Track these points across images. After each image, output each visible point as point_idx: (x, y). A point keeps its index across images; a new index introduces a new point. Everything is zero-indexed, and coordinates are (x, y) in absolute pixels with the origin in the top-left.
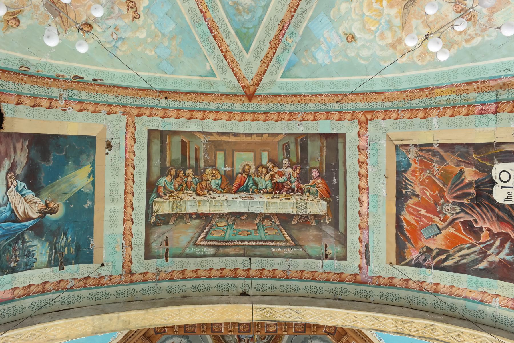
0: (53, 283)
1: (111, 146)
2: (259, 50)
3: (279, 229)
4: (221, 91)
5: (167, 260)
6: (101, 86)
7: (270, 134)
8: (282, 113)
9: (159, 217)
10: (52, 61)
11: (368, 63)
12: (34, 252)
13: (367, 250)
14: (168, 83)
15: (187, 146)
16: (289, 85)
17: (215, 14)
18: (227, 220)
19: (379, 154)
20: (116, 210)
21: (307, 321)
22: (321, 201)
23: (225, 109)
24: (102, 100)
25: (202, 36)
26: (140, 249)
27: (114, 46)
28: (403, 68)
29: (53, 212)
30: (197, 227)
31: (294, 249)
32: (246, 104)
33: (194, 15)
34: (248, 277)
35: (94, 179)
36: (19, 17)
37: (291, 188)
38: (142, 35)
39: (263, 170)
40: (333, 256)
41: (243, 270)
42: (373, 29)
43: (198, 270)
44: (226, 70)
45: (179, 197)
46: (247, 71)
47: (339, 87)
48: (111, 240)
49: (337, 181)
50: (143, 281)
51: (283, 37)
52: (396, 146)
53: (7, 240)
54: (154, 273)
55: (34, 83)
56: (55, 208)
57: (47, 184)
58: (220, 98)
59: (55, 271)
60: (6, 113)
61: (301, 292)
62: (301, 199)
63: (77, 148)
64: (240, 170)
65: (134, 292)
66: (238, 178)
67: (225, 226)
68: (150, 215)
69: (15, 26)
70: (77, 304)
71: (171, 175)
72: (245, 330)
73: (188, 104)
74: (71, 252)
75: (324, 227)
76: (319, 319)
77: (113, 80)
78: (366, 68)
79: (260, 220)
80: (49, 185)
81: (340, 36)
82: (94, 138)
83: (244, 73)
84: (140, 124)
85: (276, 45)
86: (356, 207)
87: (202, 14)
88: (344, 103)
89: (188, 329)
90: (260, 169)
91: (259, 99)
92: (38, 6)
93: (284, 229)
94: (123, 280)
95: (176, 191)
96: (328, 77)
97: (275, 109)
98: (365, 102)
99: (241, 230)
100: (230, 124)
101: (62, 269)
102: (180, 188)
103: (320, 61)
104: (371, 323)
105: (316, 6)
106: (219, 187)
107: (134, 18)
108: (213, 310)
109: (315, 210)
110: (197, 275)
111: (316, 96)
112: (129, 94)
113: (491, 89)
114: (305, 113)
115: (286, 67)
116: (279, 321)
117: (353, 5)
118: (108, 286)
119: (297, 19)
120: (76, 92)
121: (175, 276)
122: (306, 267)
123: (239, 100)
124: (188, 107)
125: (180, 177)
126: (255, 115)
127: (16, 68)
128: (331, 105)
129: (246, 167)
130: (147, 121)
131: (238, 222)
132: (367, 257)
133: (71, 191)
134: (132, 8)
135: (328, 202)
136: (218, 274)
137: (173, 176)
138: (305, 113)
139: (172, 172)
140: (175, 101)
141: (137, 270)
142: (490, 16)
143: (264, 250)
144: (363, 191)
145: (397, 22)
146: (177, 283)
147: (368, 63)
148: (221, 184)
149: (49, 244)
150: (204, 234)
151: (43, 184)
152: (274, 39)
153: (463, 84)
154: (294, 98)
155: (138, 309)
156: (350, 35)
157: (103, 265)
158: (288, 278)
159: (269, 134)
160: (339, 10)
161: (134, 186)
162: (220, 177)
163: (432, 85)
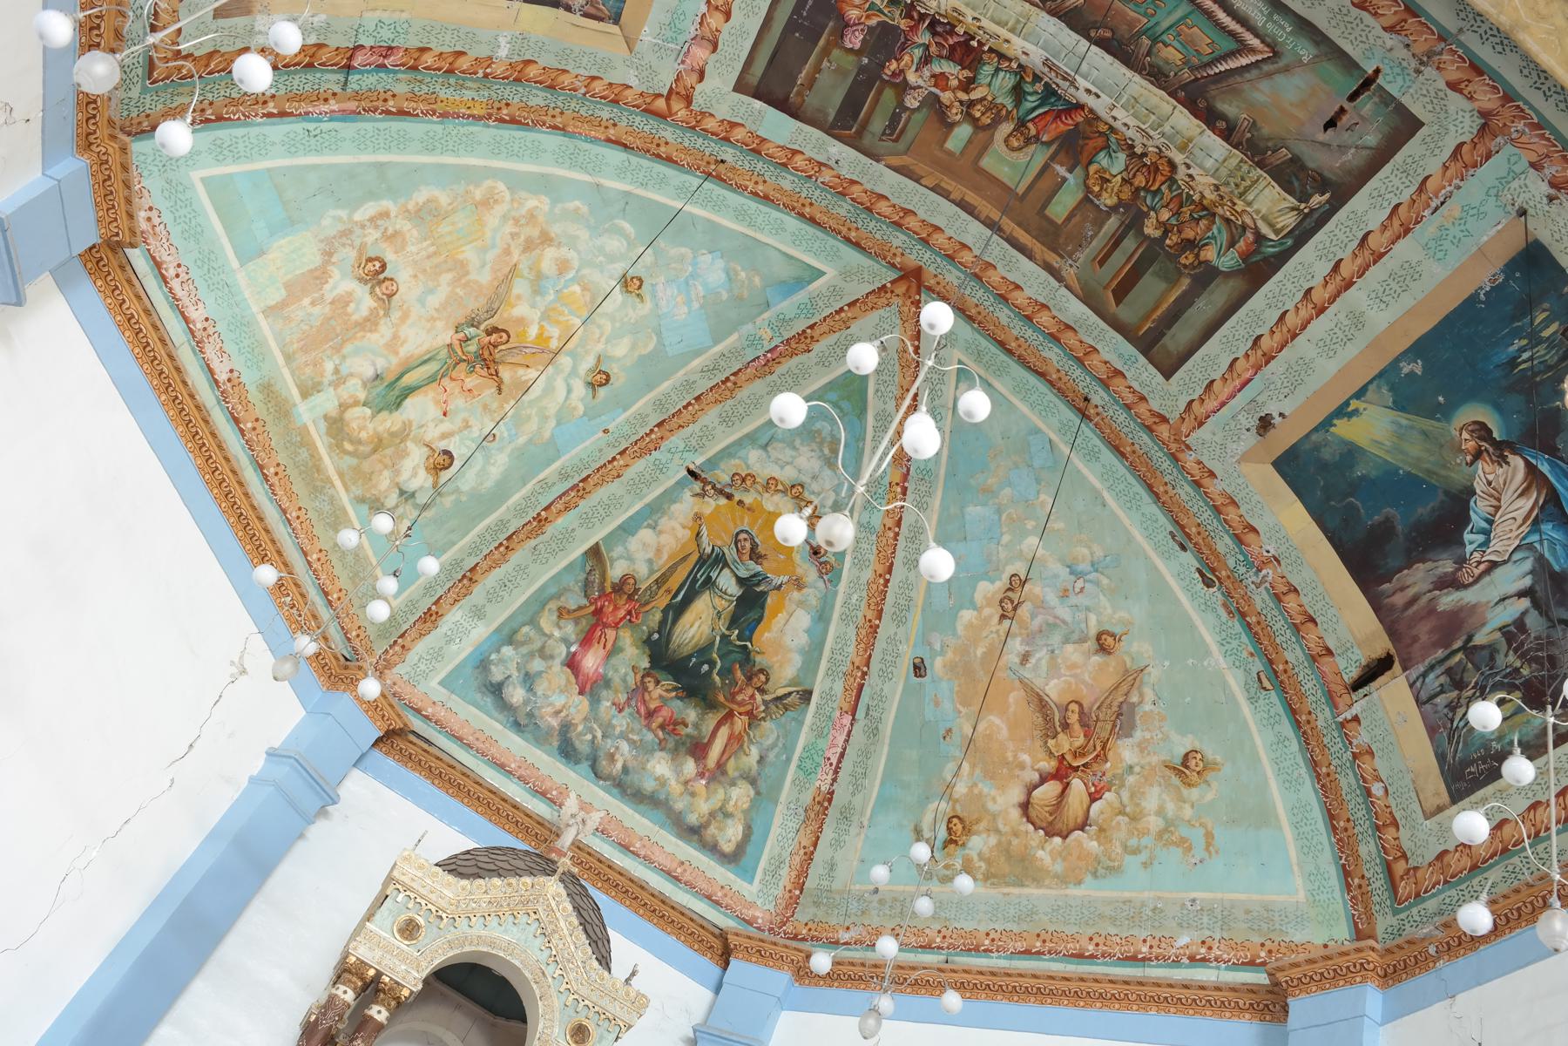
1: (1261, 419)
5: (1377, 71)
6: (1182, 527)
9: (1301, 192)
10: (1214, 648)
14: (1060, 422)
18: (1149, 54)
19: (669, 15)
20: (1373, 295)
26: (1409, 160)
27: (1097, 571)
28: (545, 185)
29: (1482, 431)
30: (1235, 92)
32: (932, 269)
35: (1351, 398)
36: (1178, 761)
37: (934, 34)
39: (978, 115)
42: (576, 288)
50: (1480, 73)
51: (777, 346)
52: (616, 20)
54: (1438, 68)
55: (1276, 646)
56: (1472, 431)
57: (1432, 488)
58: (980, 318)
68: (1316, 215)
71: (1197, 256)
73: (1053, 354)
78: (624, 210)
81: (654, 296)
82: (1278, 464)
90: (986, 120)
92: (1139, 745)
94: (1520, 125)
95: (1214, 215)
96: (720, 225)
99: (1131, 6)
103: (720, 263)
105: (677, 372)
106: (1109, 147)
107: (1023, 583)
111: (766, 198)
113: (357, 96)
117: (600, 347)
120: (1231, 563)
121: (1396, 12)
125: (1183, 236)
126: (927, 235)
127: (1273, 696)
129: (1016, 144)
133: (1412, 427)
134: (1012, 602)
137: (1196, 251)
138: (810, 177)
139: (1191, 260)
141: (1467, 115)
142: (327, 263)
145: (520, 287)
147: (616, 221)
150: (1233, 64)
151: (1441, 496)
153: (417, 115)
154: (818, 216)
159: (917, 181)
160: (634, 347)
161: (1290, 306)
162: (1092, 169)
163: (488, 126)
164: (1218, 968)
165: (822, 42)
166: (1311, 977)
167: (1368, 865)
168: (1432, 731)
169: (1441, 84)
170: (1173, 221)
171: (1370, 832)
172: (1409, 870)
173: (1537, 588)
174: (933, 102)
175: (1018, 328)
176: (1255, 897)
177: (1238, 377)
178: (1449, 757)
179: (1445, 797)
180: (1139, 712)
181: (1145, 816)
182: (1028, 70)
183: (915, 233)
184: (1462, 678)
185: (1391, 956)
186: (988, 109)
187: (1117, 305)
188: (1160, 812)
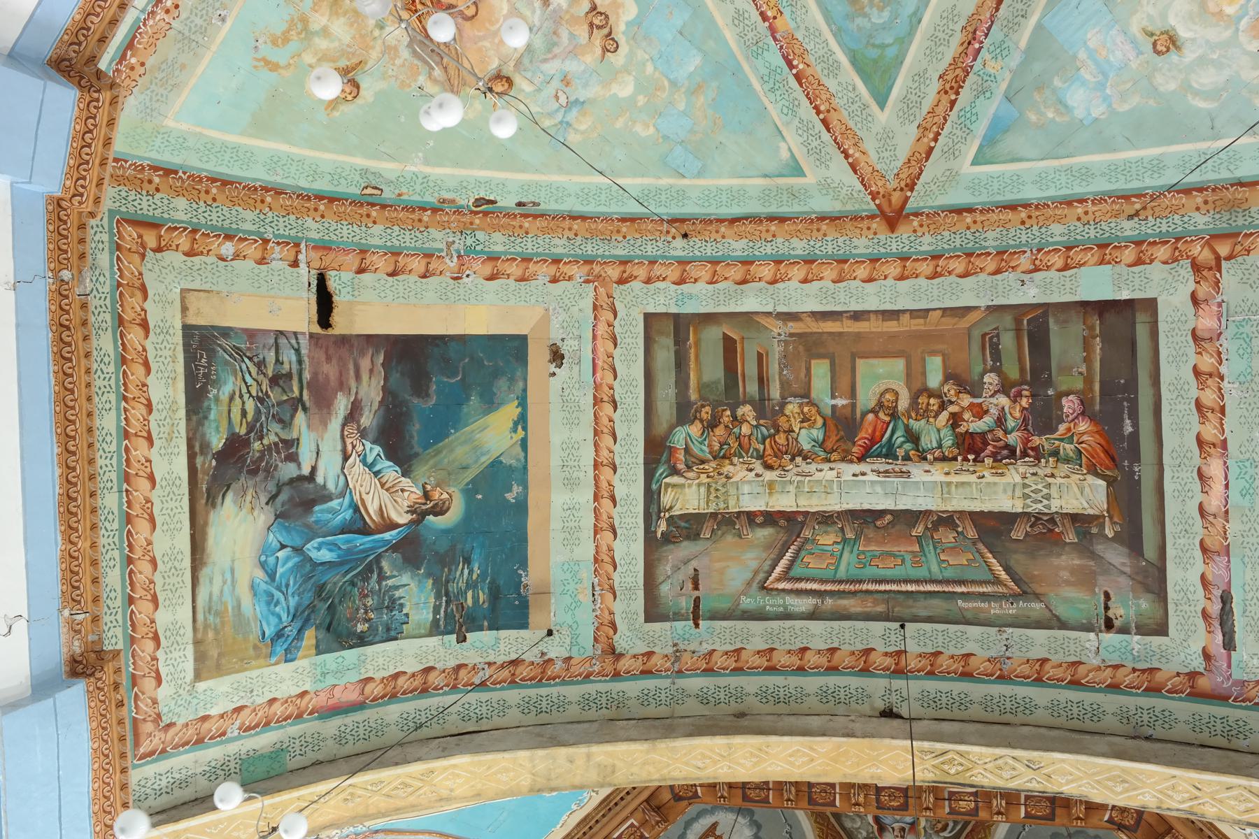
0: (444, 671)
1: (562, 357)
2: (914, 98)
3: (978, 551)
4: (817, 209)
5: (697, 625)
6: (535, 217)
7: (945, 311)
8: (979, 255)
9: (675, 523)
10: (428, 170)
11: (1216, 104)
12: (402, 601)
13: (1227, 608)
15: (739, 350)
16: (995, 180)
17: (798, 19)
18: (842, 529)
20: (577, 506)
21: (1060, 790)
22: (1091, 479)
23: (830, 253)
24: (539, 250)
25: (766, 78)
27: (561, 122)
29: (439, 510)
30: (768, 547)
31: (1018, 604)
32: (882, 237)
33: (747, 28)
34: (899, 672)
35: (526, 435)
36: (358, 79)
37: (1007, 446)
38: (625, 89)
39: (932, 401)
40: (1129, 623)
41: (886, 654)
42: (1230, 10)
43: (773, 649)
44: (828, 157)
45: (722, 474)
46: (882, 155)
47: (1134, 177)
48: (568, 575)
49: (1135, 425)
50: (643, 672)
51: (975, 60)
53: (347, 572)
55: (393, 222)
56: (444, 503)
57: (426, 448)
58: (815, 226)
59: (447, 645)
60: (337, 292)
61: (1041, 716)
62: (1034, 474)
63: (486, 363)
64: (872, 404)
65: (621, 699)
66: (866, 424)
67: (835, 543)
68: (654, 517)
69: (349, 98)
70: (497, 721)
71: (702, 421)
72: (895, 804)
73: (738, 247)
74: (481, 602)
75: (1099, 548)
76: (1093, 788)
77: (560, 201)
78: (1212, 120)
79: (927, 528)
80: (430, 450)
81: (1133, 42)
82: (523, 339)
83: (876, 161)
84: (626, 302)
85: (956, 82)
86: (1190, 494)
87: (767, 24)
88: (1150, 218)
89: (752, 794)
90: (922, 400)
91: (915, 224)
92: (396, 49)
93: (991, 552)
94: (596, 668)
95: (715, 458)
96: (1101, 152)
97: (958, 246)
98: (1212, 212)
100: (842, 290)
101: (462, 639)
102: (723, 451)
103: (1079, 113)
104: (1242, 807)
106: (820, 447)
107: (605, 50)
108: (811, 749)
109: (1075, 502)
110: (770, 664)
111: (1069, 203)
112: (599, 233)
114: (1039, 250)
115: (985, 135)
116: (982, 787)
118: (564, 683)
119: (1011, 9)
120: (481, 235)
122: (1052, 651)
123: (865, 229)
124: (739, 253)
128: (1113, 225)
129: (888, 396)
130: (641, 294)
131: (870, 532)
132: (1226, 629)
133: (476, 462)
134: (599, 27)
135: (1111, 482)
136: (823, 661)
137: (705, 423)
138: (1039, 250)
139: (703, 413)
140: (706, 241)
141: (628, 648)
143: (938, 606)
144: (1212, 451)
146: (722, 681)
147: (1216, 104)
148: (824, 440)
149: (433, 584)
150: (784, 563)
151: (417, 449)
152: (952, 67)
154: (1010, 215)
155: (631, 740)
156: (1162, 33)
157: (550, 633)
158: (1002, 678)
159: (945, 310)
162: (820, 421)
164: (143, 11)
165: (1097, 387)
166: (90, 131)
167: (166, 202)
168: (251, 334)
169: (655, 650)
170: (736, 430)
171: (195, 220)
172: (144, 248)
173: (311, 486)
174: (973, 388)
175: (780, 246)
176: (193, 81)
177: (603, 367)
178: (222, 342)
179: (192, 320)
180: (424, 70)
181: (331, 15)
182: (916, 459)
183: (917, 260)
184: (279, 386)
185: (76, 224)
186: (927, 410)
187: (724, 334)
188: (325, 32)
